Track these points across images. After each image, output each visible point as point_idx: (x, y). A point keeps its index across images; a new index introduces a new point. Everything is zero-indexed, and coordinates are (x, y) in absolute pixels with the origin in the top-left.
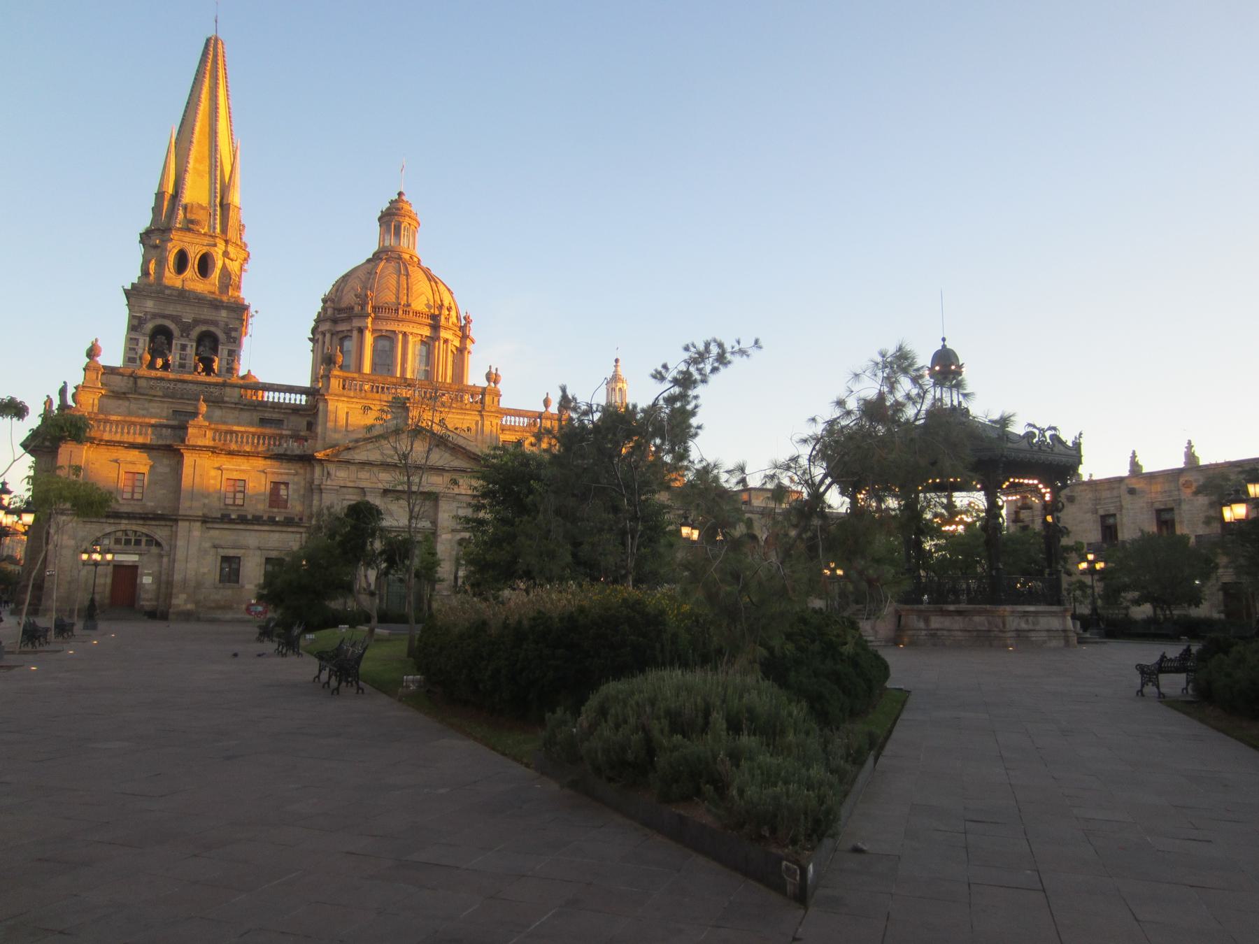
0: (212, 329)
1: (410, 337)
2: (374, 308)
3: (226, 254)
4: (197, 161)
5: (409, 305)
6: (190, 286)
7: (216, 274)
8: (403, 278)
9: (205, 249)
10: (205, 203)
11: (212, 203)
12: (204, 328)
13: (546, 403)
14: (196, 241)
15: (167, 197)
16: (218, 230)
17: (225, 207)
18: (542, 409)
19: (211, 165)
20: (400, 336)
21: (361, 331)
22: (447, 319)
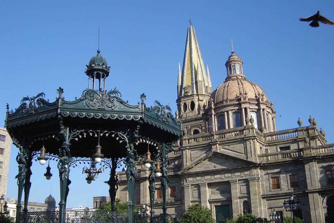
0: (197, 128)
1: (230, 112)
2: (215, 105)
3: (199, 100)
4: (187, 70)
5: (228, 98)
6: (188, 115)
7: (196, 107)
8: (226, 88)
9: (190, 101)
10: (190, 84)
11: (192, 84)
12: (194, 129)
13: (299, 123)
14: (188, 99)
15: (179, 87)
16: (195, 93)
17: (196, 83)
18: (298, 126)
19: (191, 70)
20: (226, 113)
21: (211, 116)
22: (245, 99)
